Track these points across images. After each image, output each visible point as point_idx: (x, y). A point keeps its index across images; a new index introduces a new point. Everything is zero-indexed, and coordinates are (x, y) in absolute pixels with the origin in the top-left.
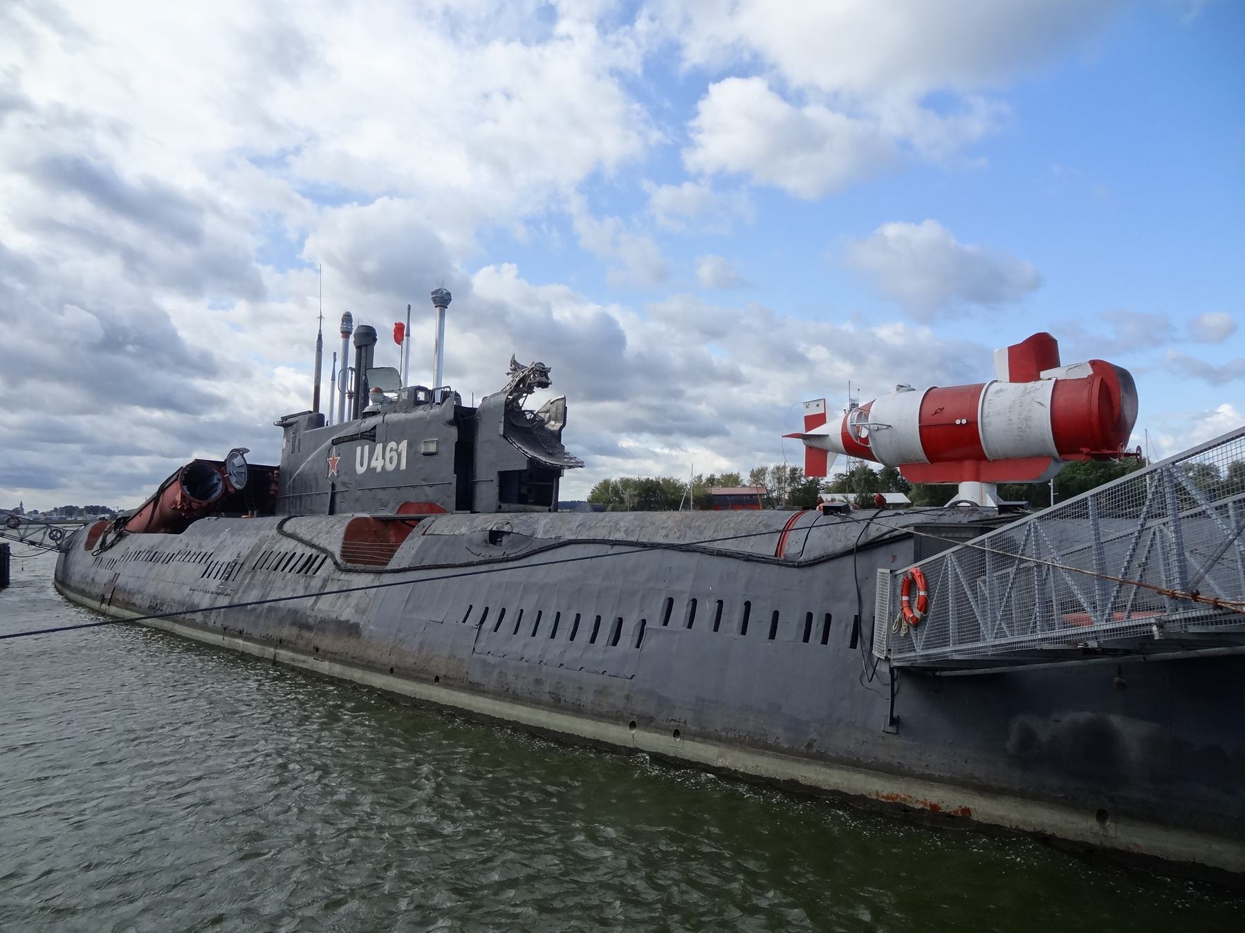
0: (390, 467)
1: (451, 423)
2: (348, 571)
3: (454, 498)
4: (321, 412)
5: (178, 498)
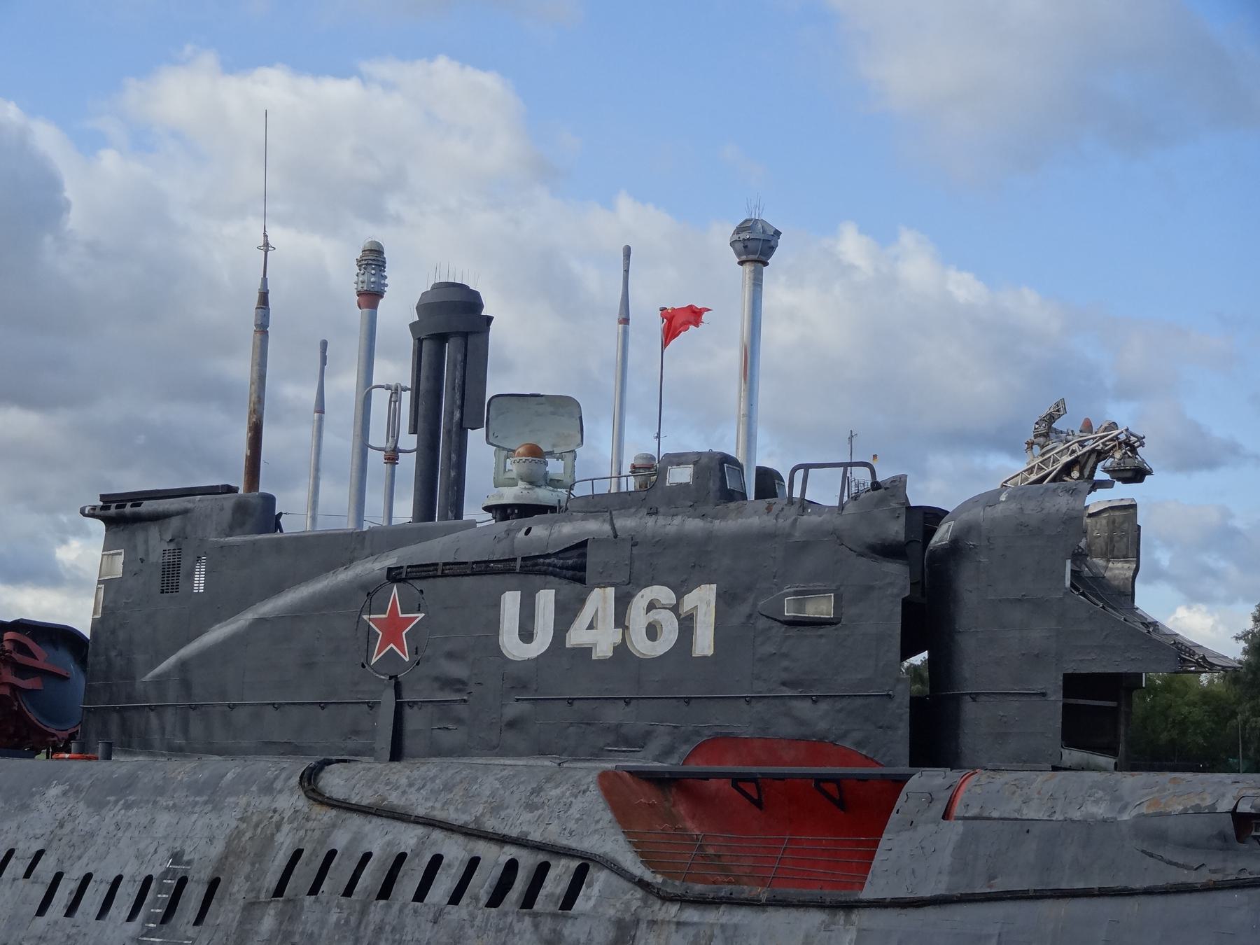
2: (684, 901)
3: (903, 730)
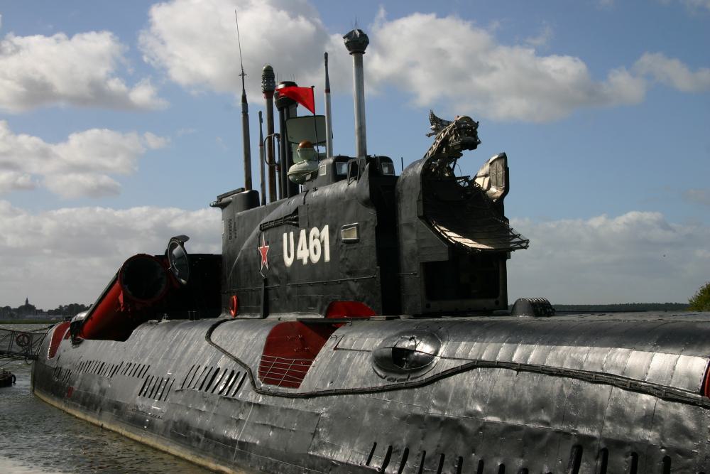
0: (316, 259)
1: (367, 203)
4: (254, 189)
5: (121, 298)
